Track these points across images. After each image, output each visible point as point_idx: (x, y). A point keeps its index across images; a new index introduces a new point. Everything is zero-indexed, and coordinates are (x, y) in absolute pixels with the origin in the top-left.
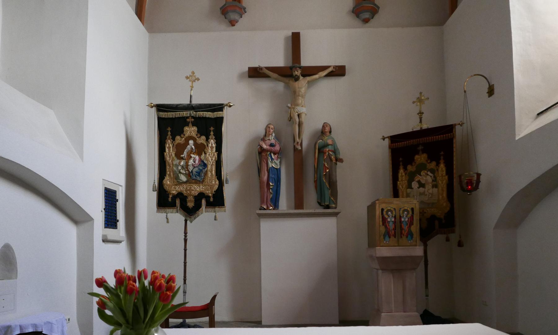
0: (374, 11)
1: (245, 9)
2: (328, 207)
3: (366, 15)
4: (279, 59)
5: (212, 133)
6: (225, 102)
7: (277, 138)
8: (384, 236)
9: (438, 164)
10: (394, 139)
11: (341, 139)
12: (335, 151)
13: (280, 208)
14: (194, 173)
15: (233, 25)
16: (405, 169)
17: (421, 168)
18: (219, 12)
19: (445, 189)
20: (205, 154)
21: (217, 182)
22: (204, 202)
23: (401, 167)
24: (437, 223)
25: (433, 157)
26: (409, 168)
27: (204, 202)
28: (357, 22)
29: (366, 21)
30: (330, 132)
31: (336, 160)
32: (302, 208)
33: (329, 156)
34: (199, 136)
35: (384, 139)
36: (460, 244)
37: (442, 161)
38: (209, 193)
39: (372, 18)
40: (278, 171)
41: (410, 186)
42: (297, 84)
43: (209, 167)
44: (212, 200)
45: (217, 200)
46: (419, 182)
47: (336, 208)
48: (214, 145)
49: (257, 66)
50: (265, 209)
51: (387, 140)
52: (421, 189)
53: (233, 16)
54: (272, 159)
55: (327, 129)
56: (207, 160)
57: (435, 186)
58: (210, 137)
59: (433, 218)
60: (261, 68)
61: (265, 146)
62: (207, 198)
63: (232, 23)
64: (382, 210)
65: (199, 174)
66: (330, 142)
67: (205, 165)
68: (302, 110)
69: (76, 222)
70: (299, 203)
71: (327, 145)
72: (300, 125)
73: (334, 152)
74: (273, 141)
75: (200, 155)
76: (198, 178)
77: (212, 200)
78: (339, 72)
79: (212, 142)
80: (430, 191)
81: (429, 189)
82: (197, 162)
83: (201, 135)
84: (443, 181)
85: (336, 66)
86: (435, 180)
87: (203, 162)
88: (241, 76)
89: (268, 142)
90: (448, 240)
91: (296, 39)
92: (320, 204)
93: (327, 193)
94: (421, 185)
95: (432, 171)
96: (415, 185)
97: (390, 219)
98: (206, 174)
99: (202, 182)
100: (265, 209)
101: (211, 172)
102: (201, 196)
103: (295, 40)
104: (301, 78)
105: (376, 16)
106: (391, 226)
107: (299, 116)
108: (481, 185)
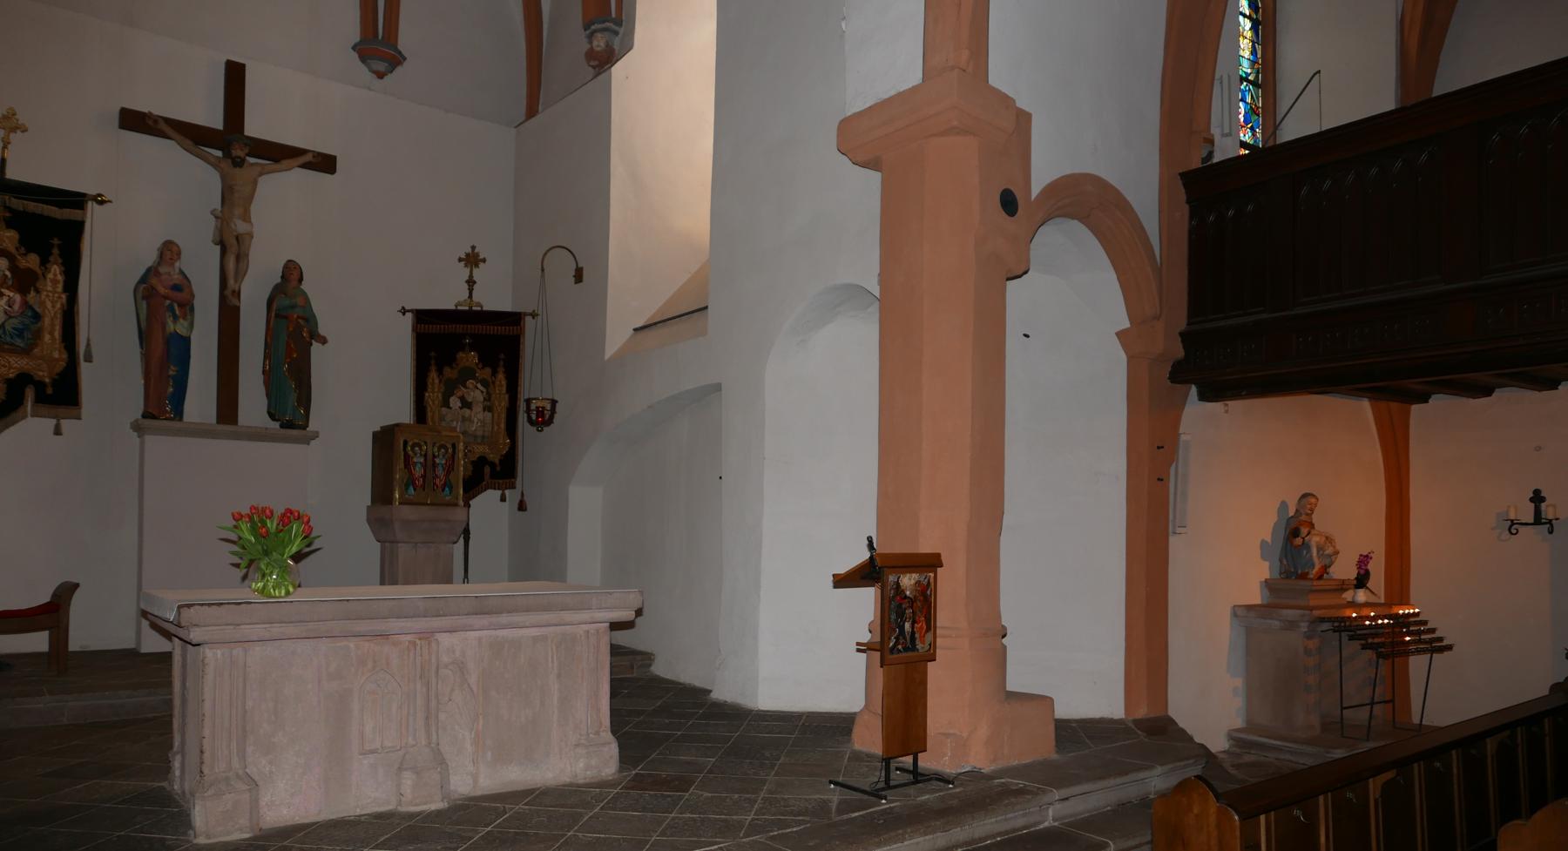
0: (396, 60)
3: (381, 66)
5: (56, 251)
6: (91, 190)
9: (494, 373)
10: (423, 318)
13: (185, 418)
14: (8, 327)
16: (440, 372)
17: (468, 374)
19: (503, 416)
20: (38, 291)
21: (65, 356)
22: (30, 394)
23: (433, 368)
24: (487, 469)
25: (487, 360)
26: (447, 370)
27: (30, 394)
29: (381, 76)
30: (301, 280)
34: (23, 250)
35: (404, 311)
36: (522, 507)
37: (501, 370)
38: (44, 375)
40: (186, 341)
41: (446, 404)
43: (47, 321)
44: (50, 391)
45: (62, 394)
46: (462, 399)
48: (60, 278)
51: (409, 315)
52: (467, 412)
54: (175, 318)
55: (295, 276)
56: (43, 303)
57: (488, 409)
58: (51, 259)
59: (480, 463)
61: (162, 290)
62: (40, 386)
64: (406, 443)
65: (20, 333)
66: (299, 301)
67: (37, 317)
73: (306, 320)
74: (176, 278)
75: (23, 291)
76: (19, 342)
77: (50, 391)
79: (56, 271)
80: (480, 416)
81: (478, 415)
82: (16, 307)
83: (29, 250)
84: (502, 403)
85: (319, 154)
86: (488, 398)
87: (31, 308)
90: (503, 499)
91: (235, 75)
92: (272, 416)
94: (466, 404)
95: (485, 383)
96: (455, 402)
98: (38, 335)
99: (26, 352)
101: (52, 333)
102: (24, 379)
105: (399, 69)
106: (418, 471)
108: (557, 418)
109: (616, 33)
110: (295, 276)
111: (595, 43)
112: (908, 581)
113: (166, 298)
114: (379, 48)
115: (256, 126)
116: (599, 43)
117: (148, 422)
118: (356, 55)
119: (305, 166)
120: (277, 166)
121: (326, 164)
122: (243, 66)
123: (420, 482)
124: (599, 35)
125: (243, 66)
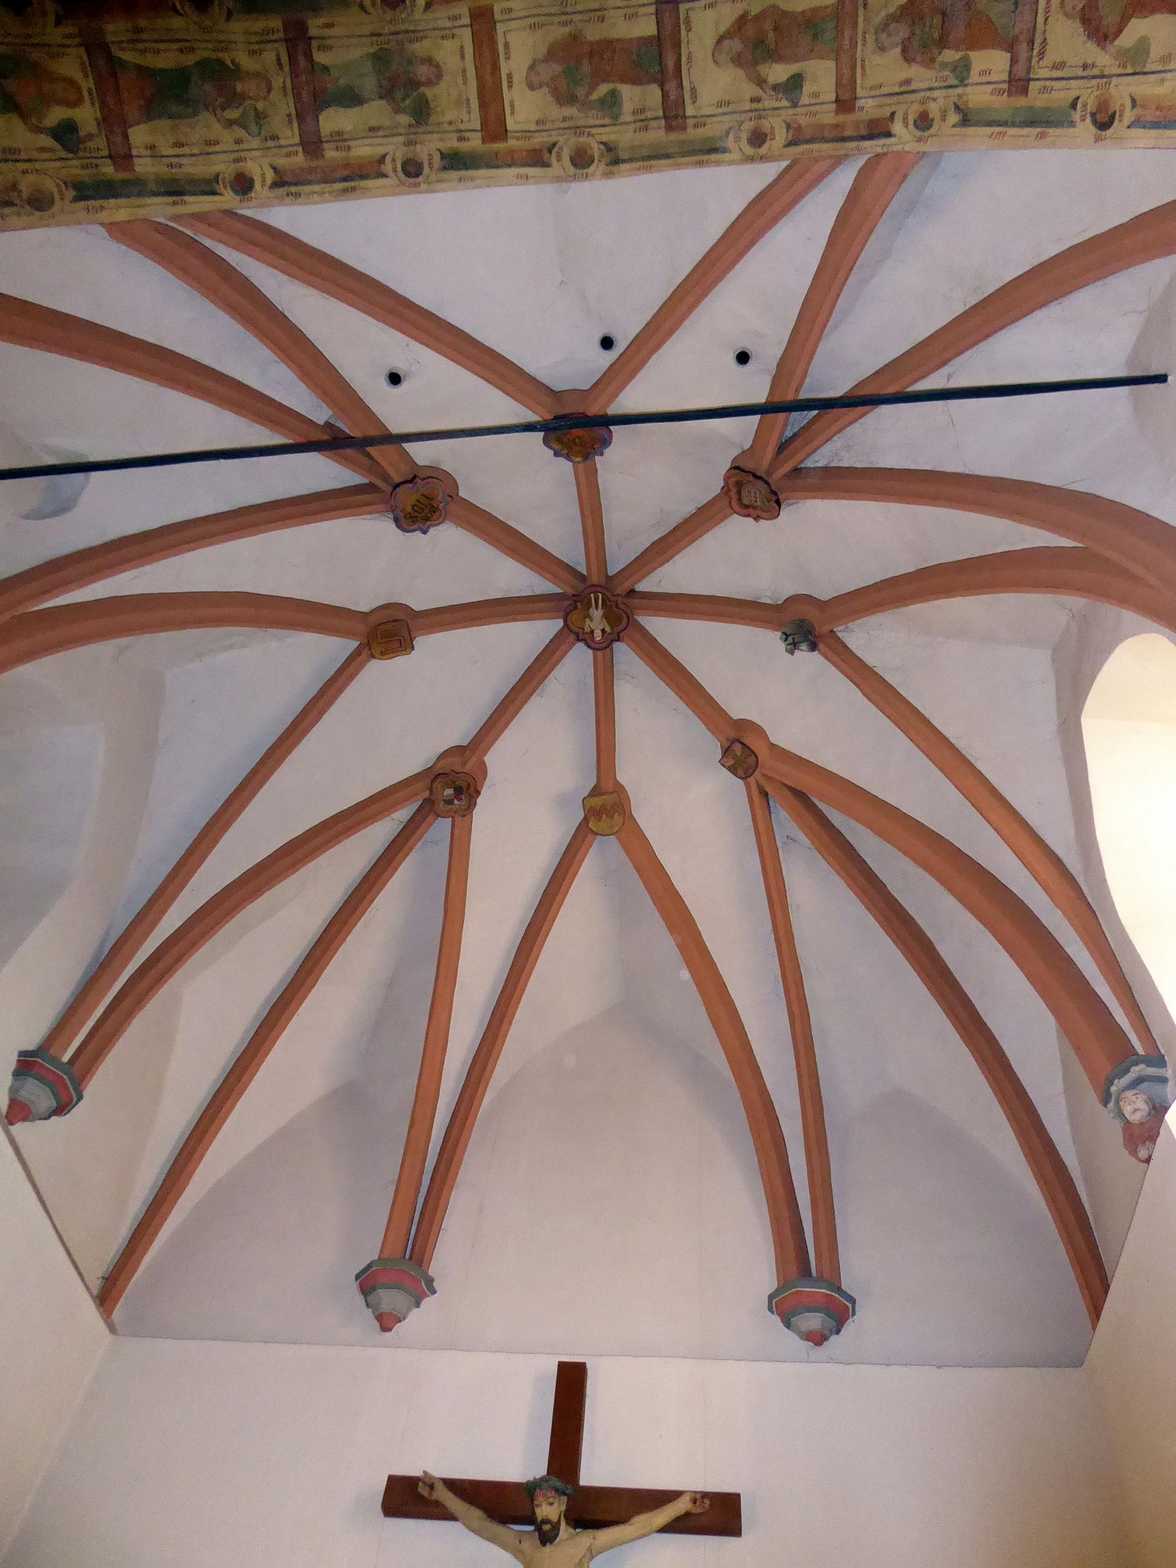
0: (839, 1312)
1: (430, 1281)
3: (814, 1321)
15: (385, 1329)
18: (355, 1286)
29: (818, 1339)
39: (838, 1332)
49: (418, 1473)
53: (389, 1299)
60: (429, 1482)
78: (718, 1515)
85: (705, 1495)
91: (571, 1383)
104: (564, 1530)
109: (1163, 1080)
111: (1127, 1110)
114: (811, 1293)
115: (598, 1469)
116: (1135, 1107)
118: (776, 1319)
122: (584, 1364)
124: (1129, 1094)
125: (584, 1364)
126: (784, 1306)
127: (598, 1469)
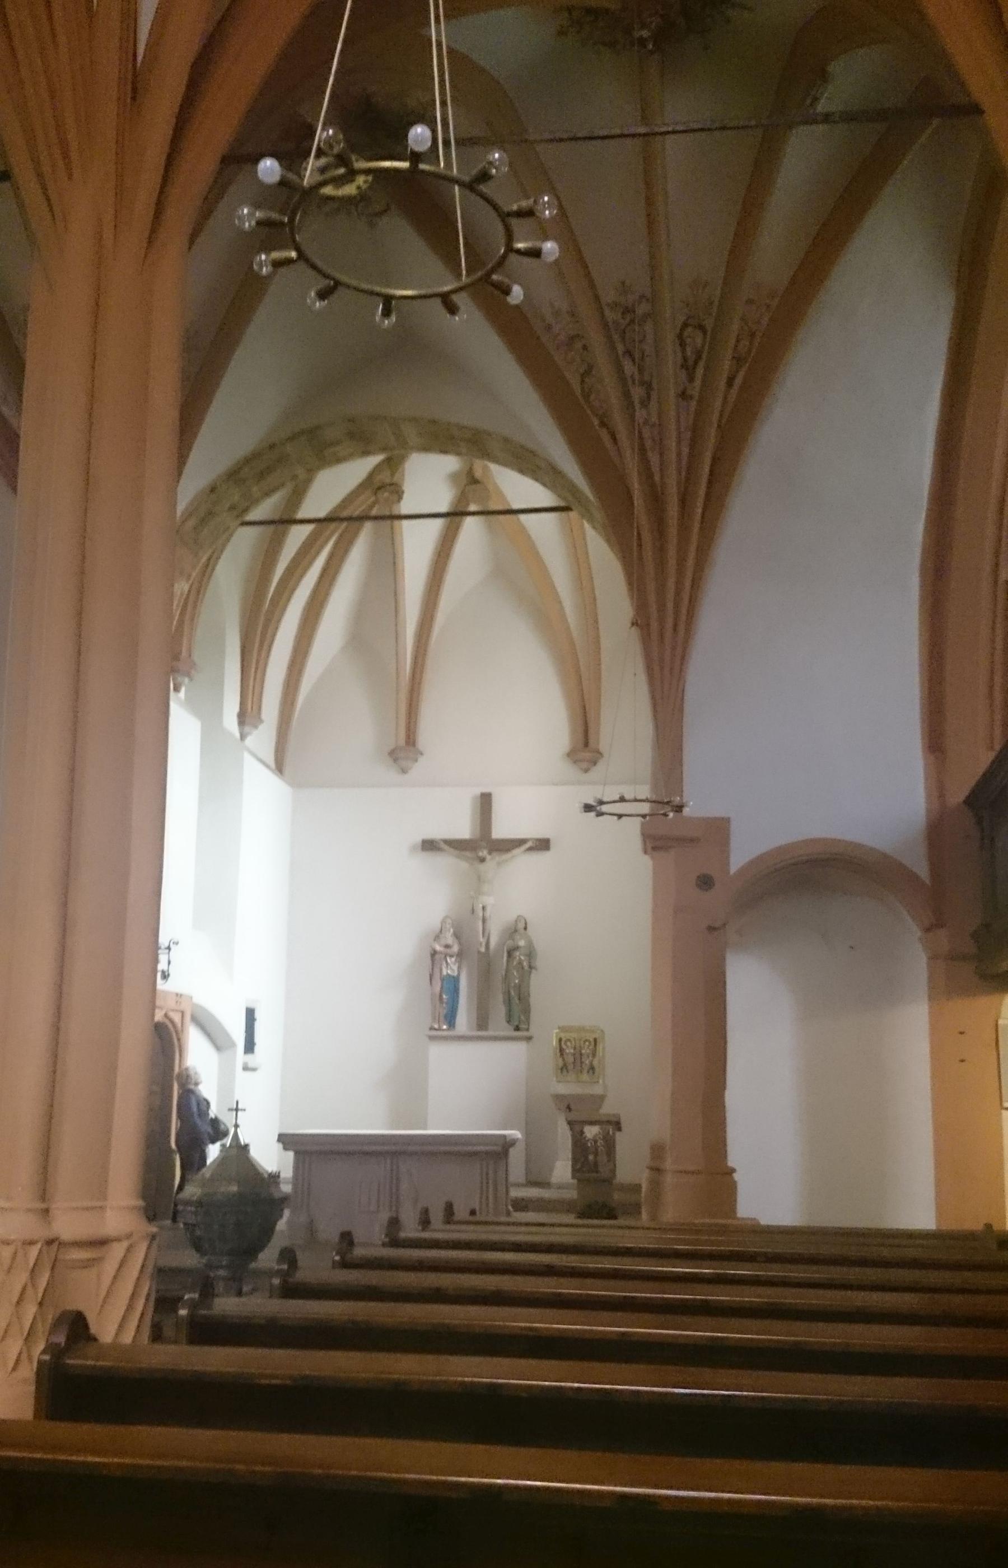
2: (517, 1029)
3: (585, 765)
4: (463, 829)
7: (457, 936)
8: (562, 1069)
11: (540, 937)
12: (531, 954)
28: (570, 771)
29: (586, 771)
30: (525, 929)
31: (530, 967)
32: (486, 1029)
33: (520, 963)
40: (455, 981)
42: (482, 867)
47: (528, 1030)
50: (436, 1029)
61: (438, 948)
63: (404, 771)
64: (560, 1040)
66: (522, 943)
68: (489, 900)
69: (218, 1048)
70: (482, 1022)
71: (517, 948)
72: (484, 921)
78: (543, 845)
88: (413, 849)
89: (443, 942)
93: (516, 1008)
97: (570, 1051)
100: (436, 1029)
103: (485, 801)
104: (488, 857)
107: (484, 908)
110: (521, 926)
112: (591, 1132)
113: (441, 953)
117: (434, 1033)
119: (530, 849)
120: (508, 855)
121: (543, 845)
123: (571, 1067)
126: (572, 755)
127: (500, 831)
